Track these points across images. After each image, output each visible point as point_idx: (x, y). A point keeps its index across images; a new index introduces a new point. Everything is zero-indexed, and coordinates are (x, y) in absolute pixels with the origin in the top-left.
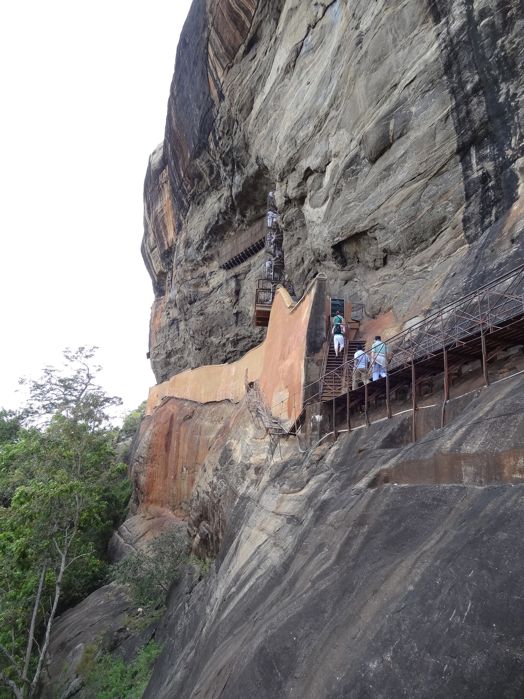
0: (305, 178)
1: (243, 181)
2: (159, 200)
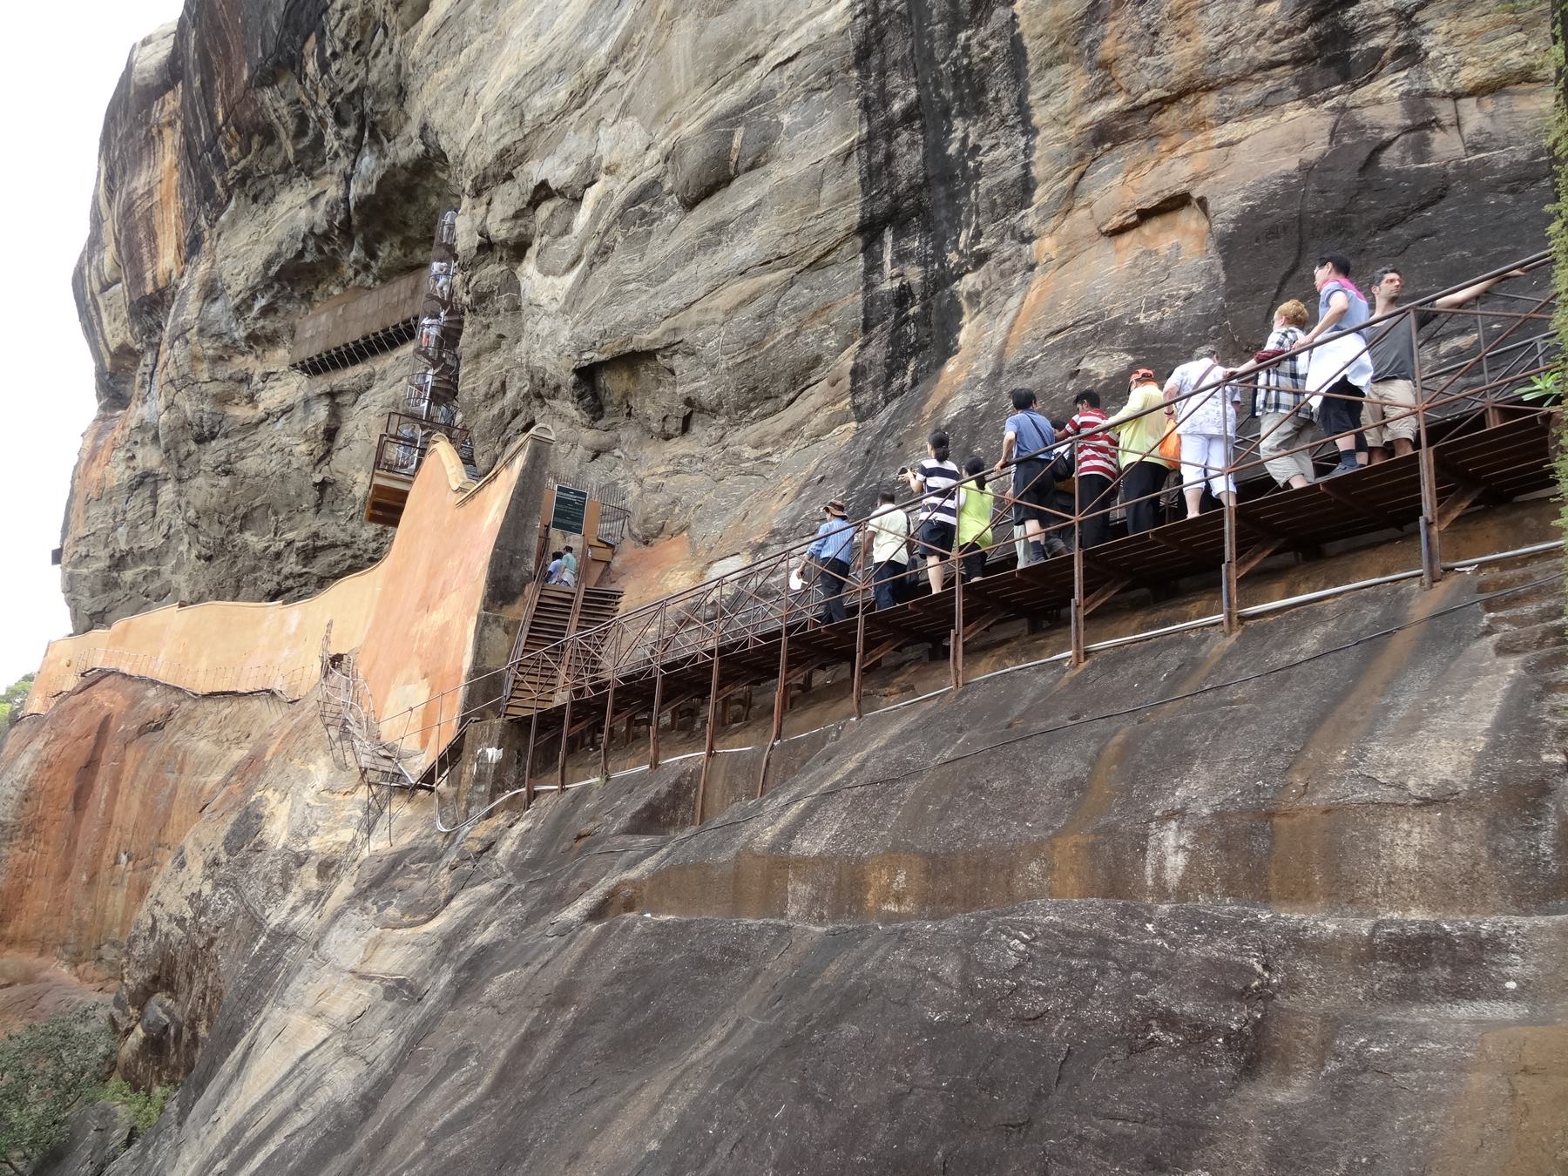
0: (534, 204)
1: (380, 173)
2: (145, 163)
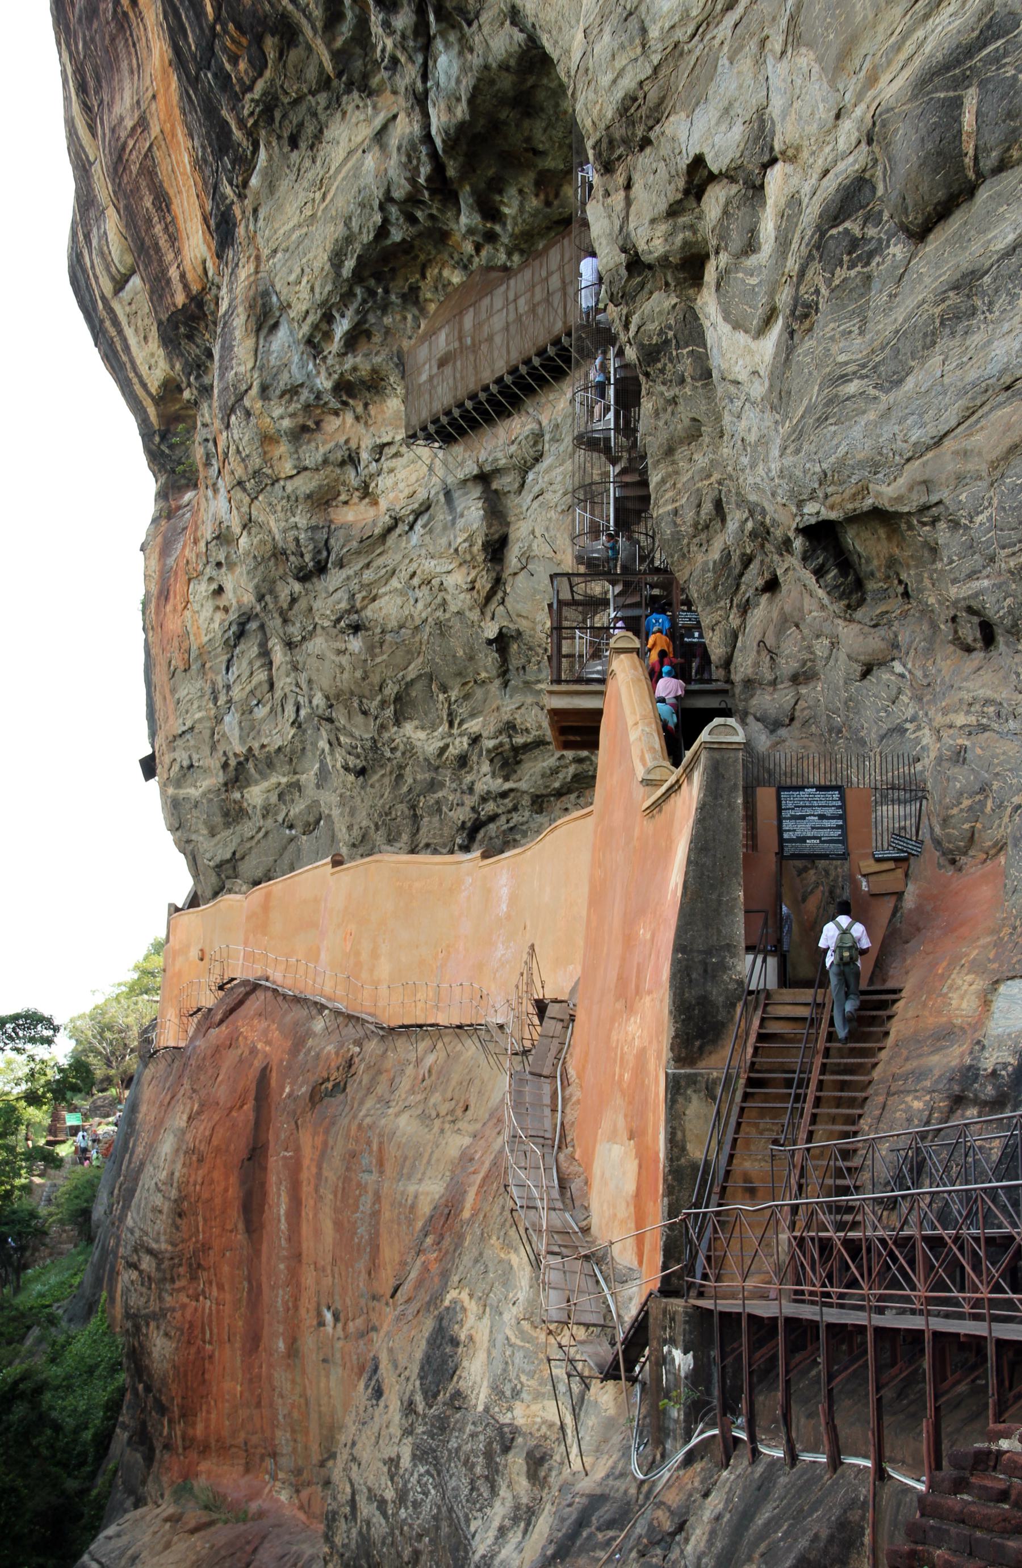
1: (468, 82)
2: (124, 66)
